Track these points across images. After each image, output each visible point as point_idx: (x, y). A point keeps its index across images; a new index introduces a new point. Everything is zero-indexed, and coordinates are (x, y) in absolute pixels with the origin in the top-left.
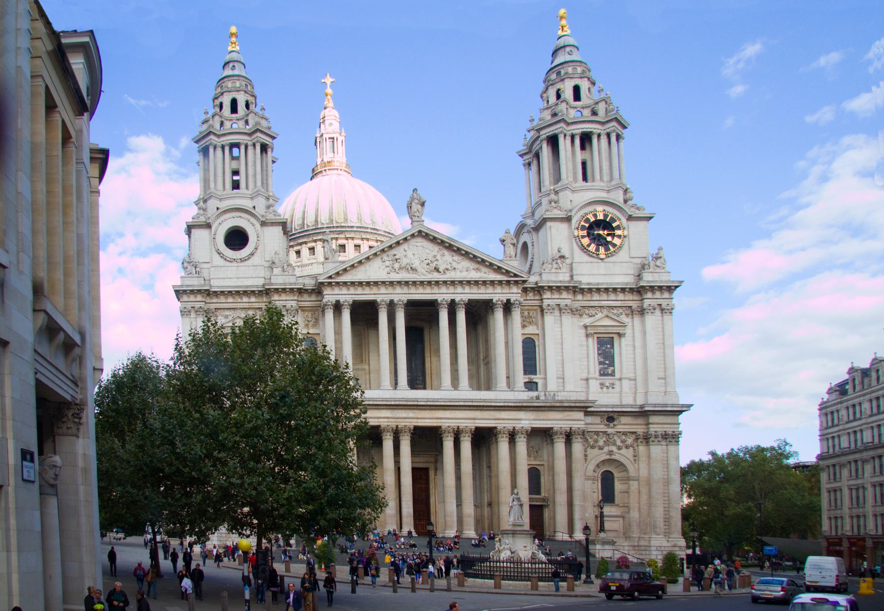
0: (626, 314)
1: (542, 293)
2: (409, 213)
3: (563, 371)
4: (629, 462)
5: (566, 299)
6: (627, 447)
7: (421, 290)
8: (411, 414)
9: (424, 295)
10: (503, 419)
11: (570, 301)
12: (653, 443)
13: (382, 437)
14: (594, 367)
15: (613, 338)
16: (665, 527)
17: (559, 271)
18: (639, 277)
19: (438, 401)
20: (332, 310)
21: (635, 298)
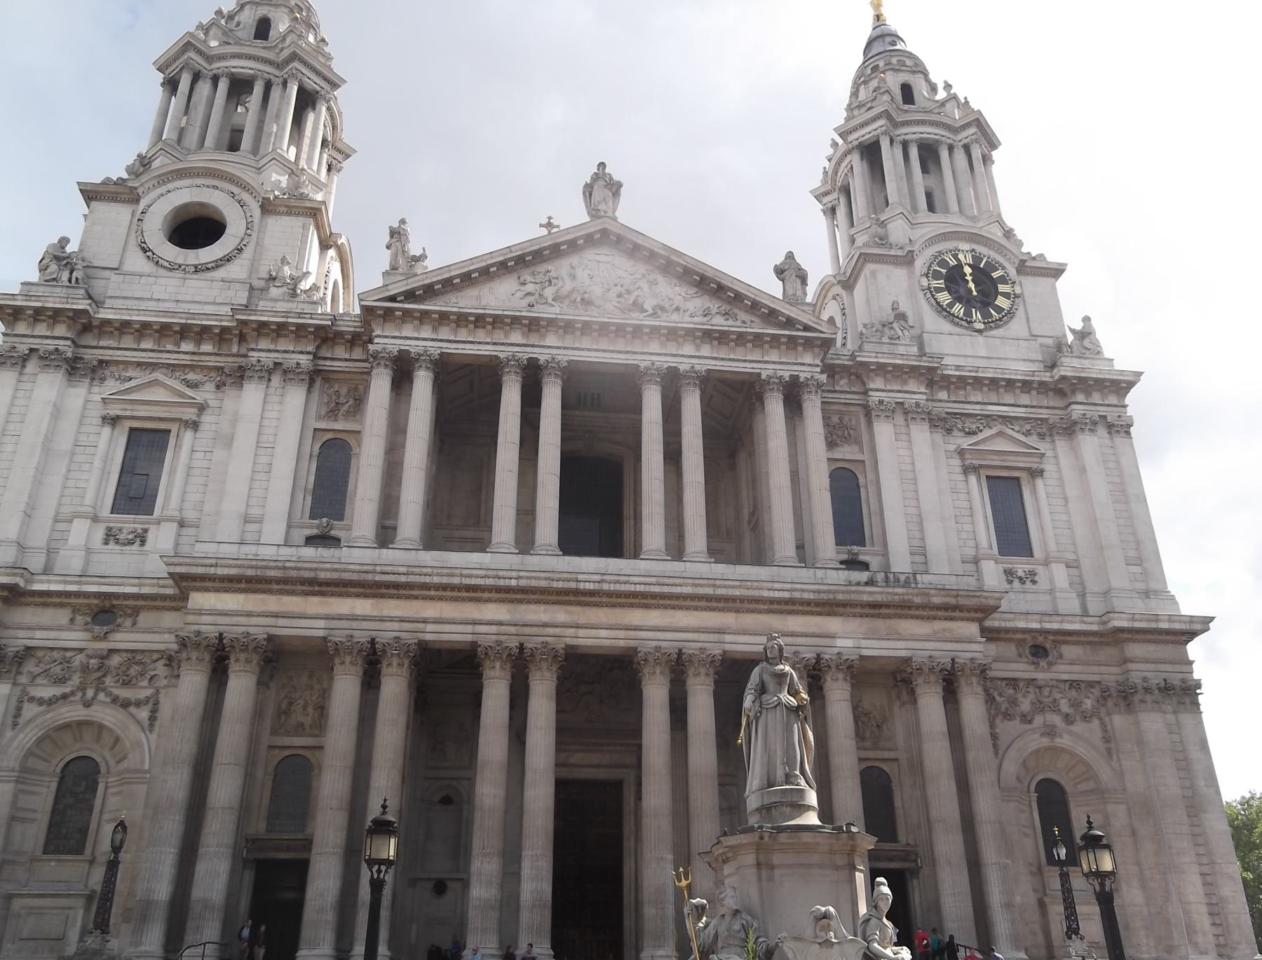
0: (1039, 434)
1: (865, 380)
2: (586, 206)
3: (923, 539)
5: (916, 392)
6: (1086, 718)
7: (604, 345)
8: (560, 614)
9: (608, 355)
11: (925, 397)
13: (480, 676)
14: (985, 534)
16: (1219, 931)
17: (897, 342)
18: (1053, 366)
21: (1051, 404)
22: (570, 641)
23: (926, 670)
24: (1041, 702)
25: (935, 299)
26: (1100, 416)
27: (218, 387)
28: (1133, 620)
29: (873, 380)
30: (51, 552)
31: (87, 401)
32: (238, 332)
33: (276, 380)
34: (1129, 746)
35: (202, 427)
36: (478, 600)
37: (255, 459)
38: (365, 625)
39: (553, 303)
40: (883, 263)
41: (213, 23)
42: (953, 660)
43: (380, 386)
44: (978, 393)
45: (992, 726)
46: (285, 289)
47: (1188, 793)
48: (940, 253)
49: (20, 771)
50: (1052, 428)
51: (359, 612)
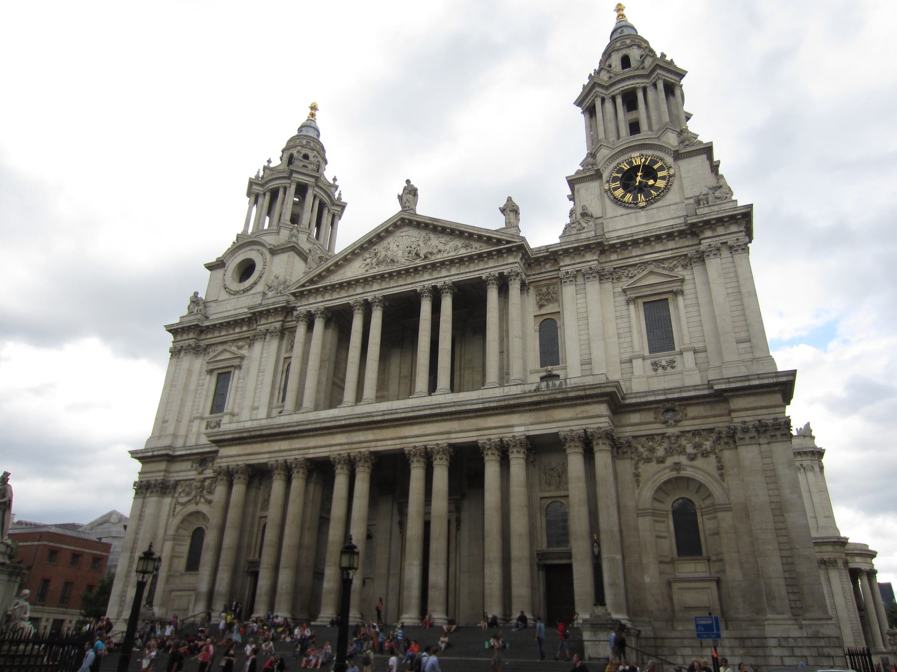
0: (683, 266)
4: (709, 478)
5: (591, 260)
6: (705, 454)
7: (401, 282)
8: (369, 435)
9: (402, 288)
10: (489, 429)
12: (742, 442)
14: (639, 340)
15: (667, 299)
16: (792, 597)
17: (584, 231)
19: (396, 413)
20: (304, 323)
21: (691, 243)
22: (372, 449)
23: (569, 439)
24: (670, 448)
25: (613, 196)
26: (722, 243)
27: (249, 346)
28: (729, 382)
29: (563, 260)
30: (187, 436)
31: (202, 365)
32: (253, 318)
33: (268, 337)
34: (735, 470)
35: (244, 367)
36: (332, 434)
37: (257, 378)
38: (285, 454)
39: (377, 267)
40: (584, 182)
41: (265, 168)
42: (585, 430)
43: (301, 330)
44: (638, 249)
45: (636, 468)
46: (274, 292)
47: (773, 499)
48: (619, 164)
49: (174, 535)
50: (691, 259)
51: (283, 448)
